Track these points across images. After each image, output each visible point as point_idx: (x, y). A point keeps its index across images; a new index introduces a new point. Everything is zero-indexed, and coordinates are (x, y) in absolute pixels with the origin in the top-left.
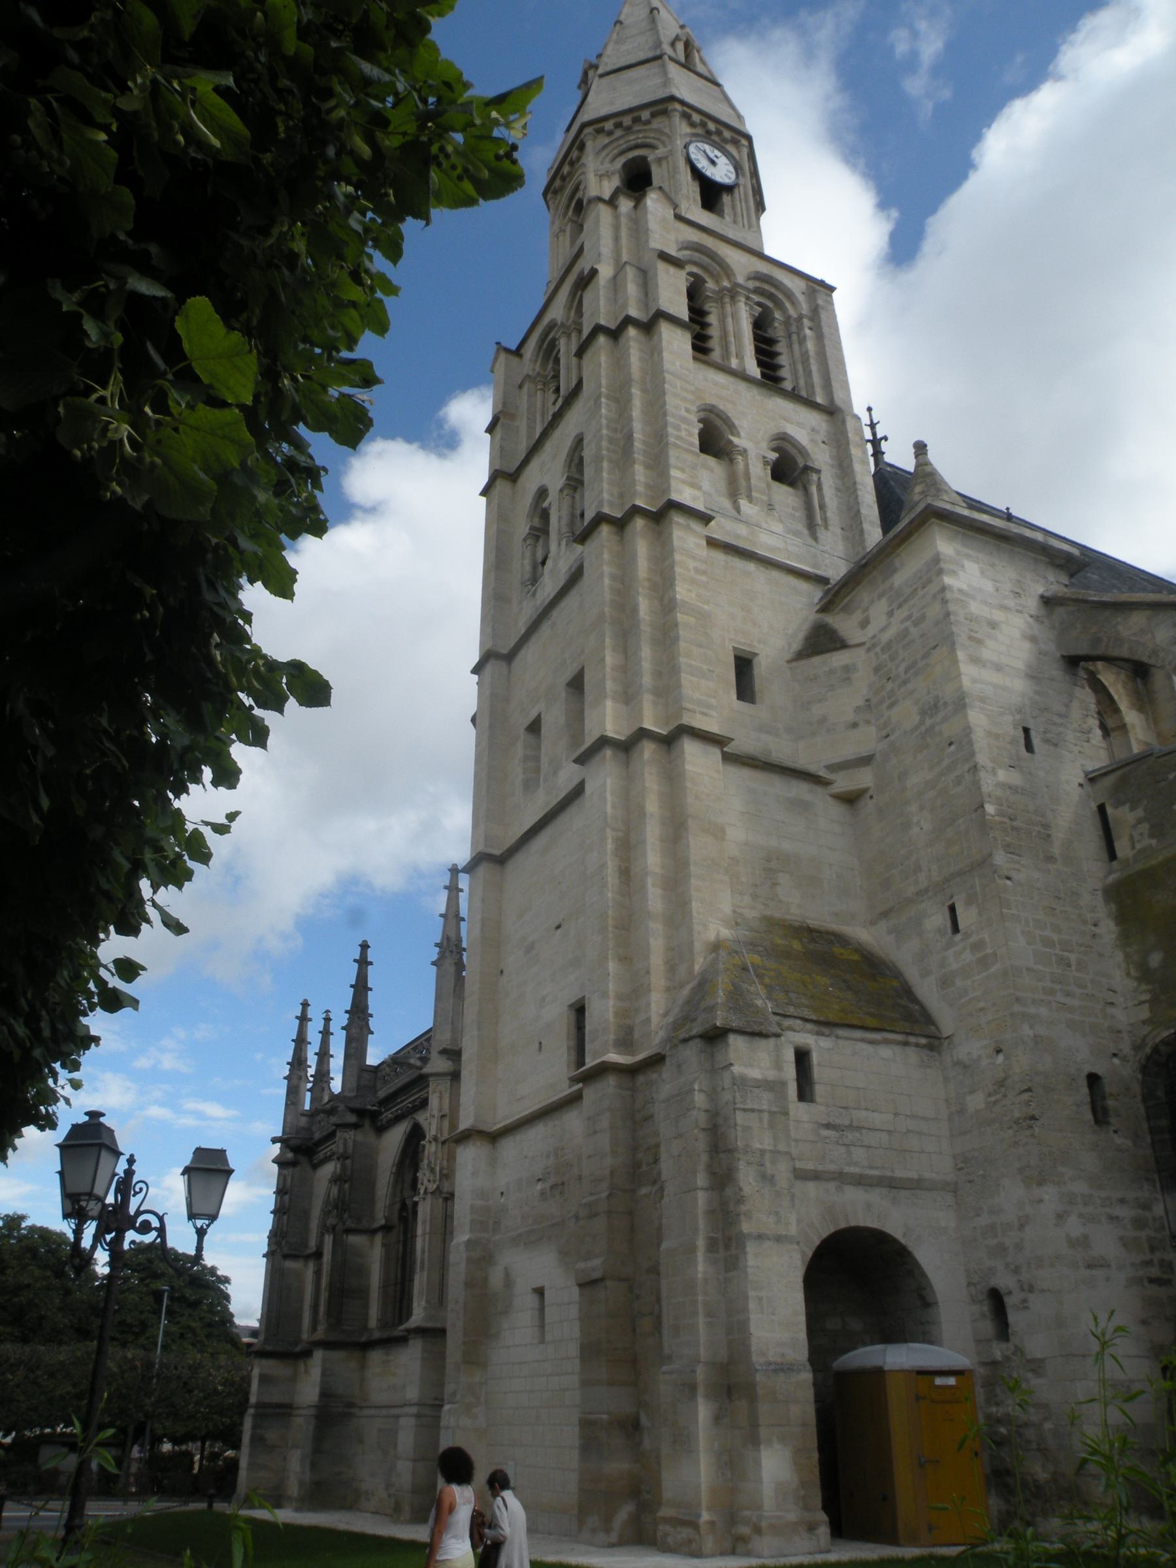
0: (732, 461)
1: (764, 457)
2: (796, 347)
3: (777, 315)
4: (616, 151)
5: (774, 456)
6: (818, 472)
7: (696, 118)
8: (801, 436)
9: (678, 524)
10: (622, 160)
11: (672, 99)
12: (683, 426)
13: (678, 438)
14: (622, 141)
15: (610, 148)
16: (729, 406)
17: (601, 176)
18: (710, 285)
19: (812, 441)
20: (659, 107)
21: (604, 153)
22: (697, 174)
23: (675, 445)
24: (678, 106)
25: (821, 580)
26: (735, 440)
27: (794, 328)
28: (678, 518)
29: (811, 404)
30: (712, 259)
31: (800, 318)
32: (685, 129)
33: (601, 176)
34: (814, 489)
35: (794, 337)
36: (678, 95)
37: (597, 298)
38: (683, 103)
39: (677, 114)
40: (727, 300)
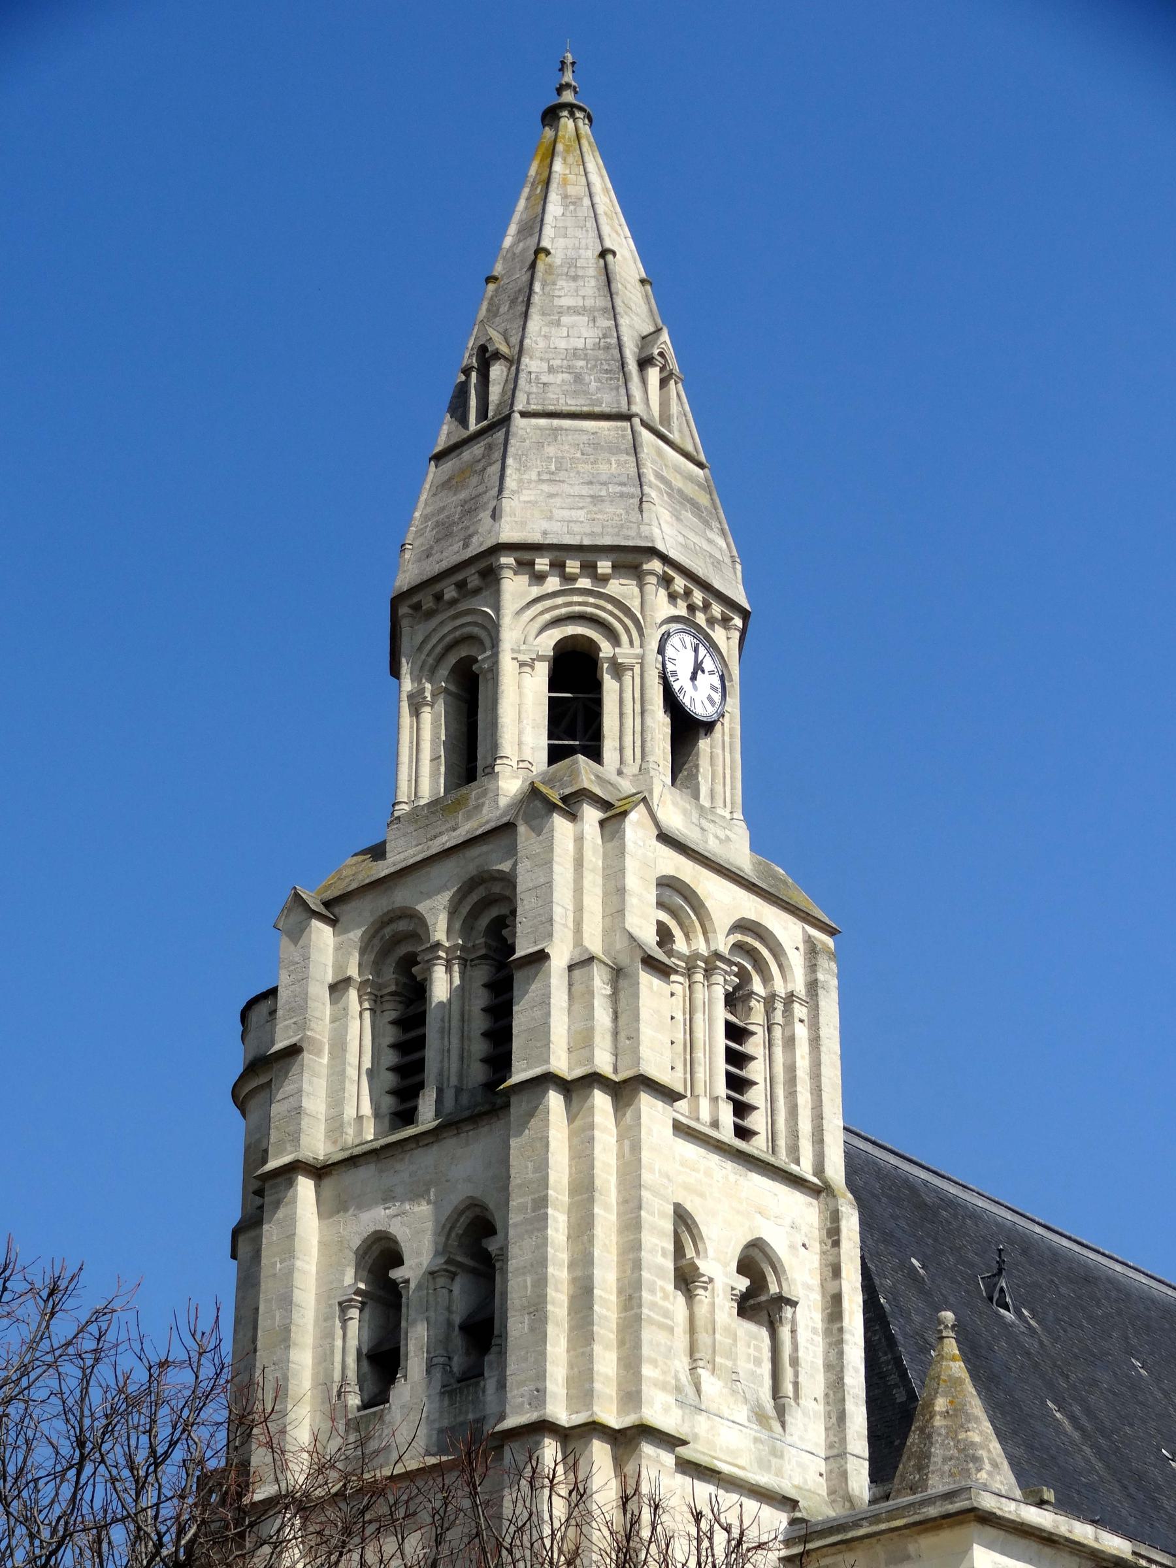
0: (690, 1296)
1: (733, 1289)
2: (778, 1051)
3: (757, 986)
4: (548, 616)
5: (743, 1284)
6: (794, 1304)
7: (680, 583)
8: (779, 1244)
9: (649, 1456)
10: (556, 634)
11: (653, 552)
12: (660, 1283)
13: (653, 1305)
14: (560, 600)
15: (539, 607)
16: (698, 1200)
17: (522, 665)
18: (680, 944)
19: (792, 1247)
20: (630, 558)
21: (530, 613)
22: (672, 703)
23: (652, 1322)
24: (656, 565)
25: (787, 1503)
26: (704, 1266)
27: (778, 1017)
28: (648, 1449)
29: (796, 1181)
30: (686, 899)
31: (790, 998)
32: (661, 607)
33: (522, 665)
34: (785, 1332)
35: (778, 1032)
36: (660, 546)
37: (545, 1002)
38: (665, 559)
39: (652, 580)
40: (699, 977)
